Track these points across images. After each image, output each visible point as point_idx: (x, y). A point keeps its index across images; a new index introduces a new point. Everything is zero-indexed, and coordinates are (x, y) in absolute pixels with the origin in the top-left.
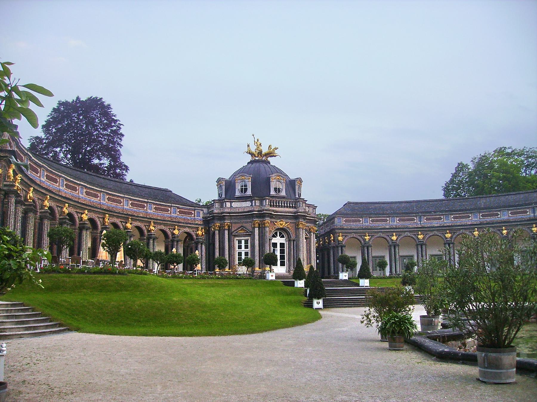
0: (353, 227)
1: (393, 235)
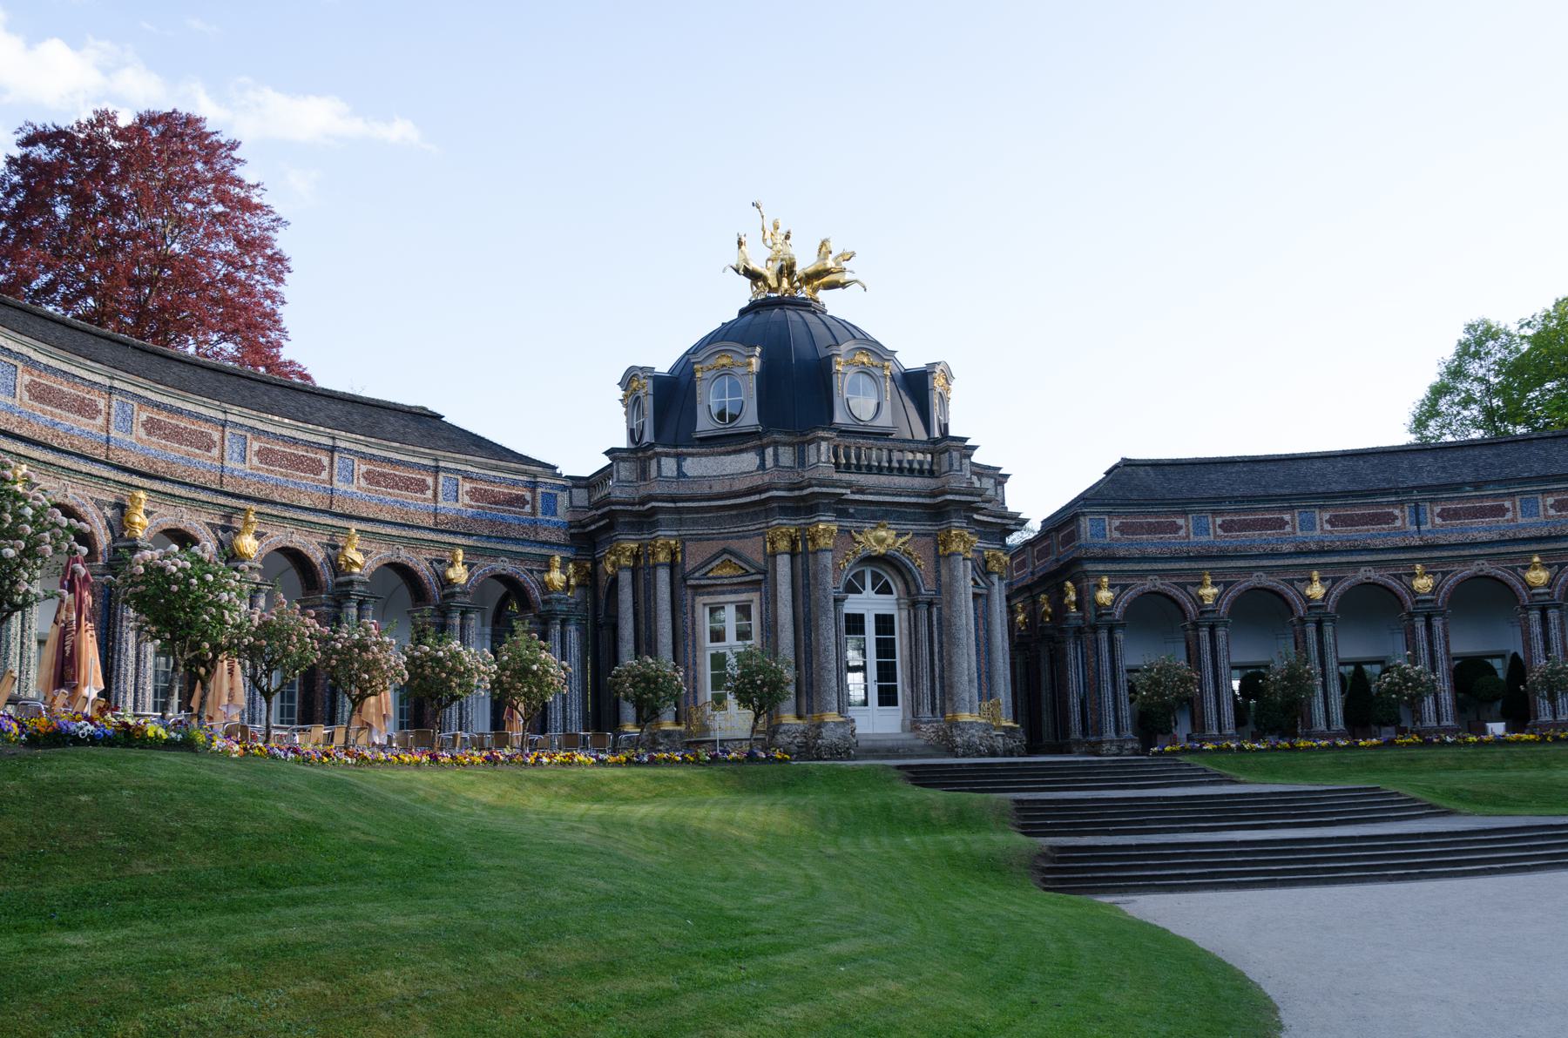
0: (1151, 550)
1: (1311, 580)
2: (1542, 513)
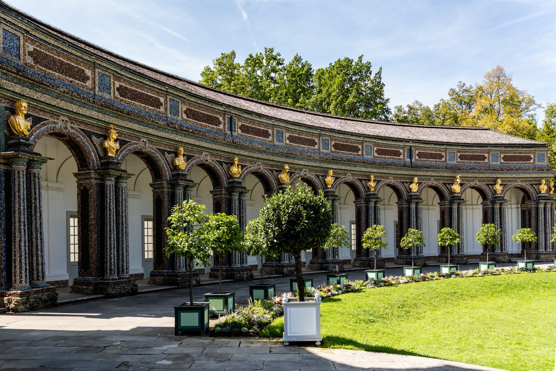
2: (284, 141)
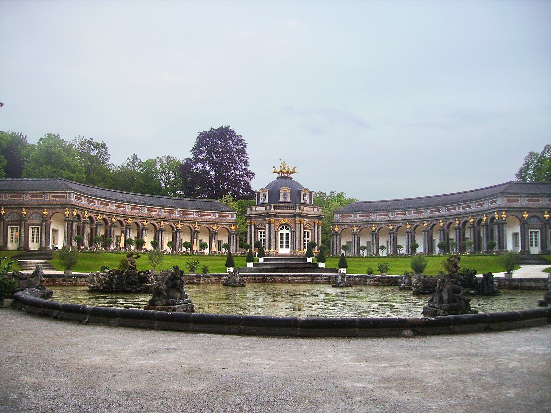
0: (346, 221)
